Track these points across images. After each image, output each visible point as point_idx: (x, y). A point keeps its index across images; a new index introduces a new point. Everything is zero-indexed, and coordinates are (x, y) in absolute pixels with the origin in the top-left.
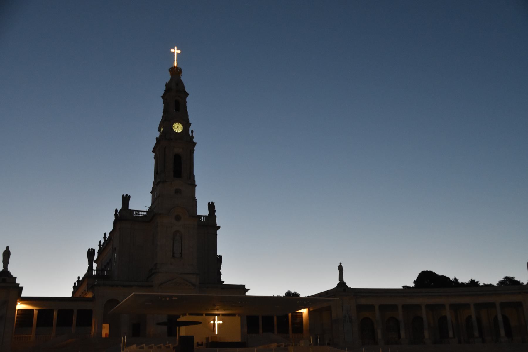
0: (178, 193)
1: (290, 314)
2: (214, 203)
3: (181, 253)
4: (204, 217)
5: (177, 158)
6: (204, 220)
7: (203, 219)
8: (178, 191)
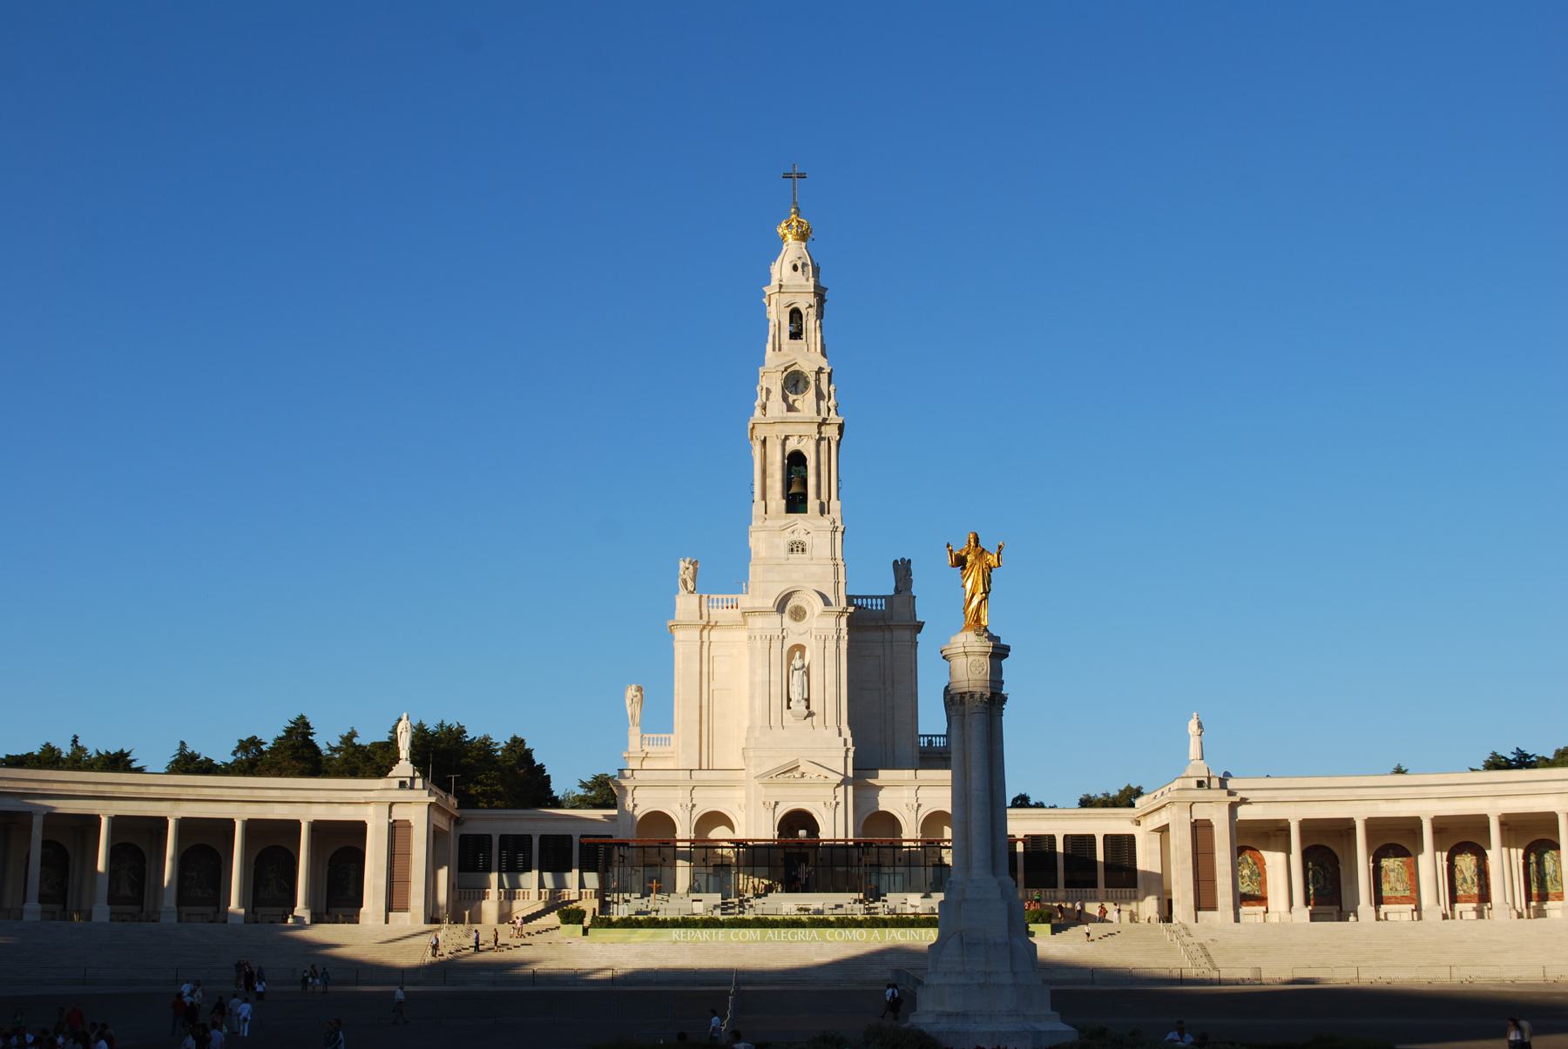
0: (798, 551)
1: (467, 913)
2: (909, 561)
3: (808, 700)
4: (883, 600)
6: (884, 608)
7: (881, 605)
8: (797, 547)
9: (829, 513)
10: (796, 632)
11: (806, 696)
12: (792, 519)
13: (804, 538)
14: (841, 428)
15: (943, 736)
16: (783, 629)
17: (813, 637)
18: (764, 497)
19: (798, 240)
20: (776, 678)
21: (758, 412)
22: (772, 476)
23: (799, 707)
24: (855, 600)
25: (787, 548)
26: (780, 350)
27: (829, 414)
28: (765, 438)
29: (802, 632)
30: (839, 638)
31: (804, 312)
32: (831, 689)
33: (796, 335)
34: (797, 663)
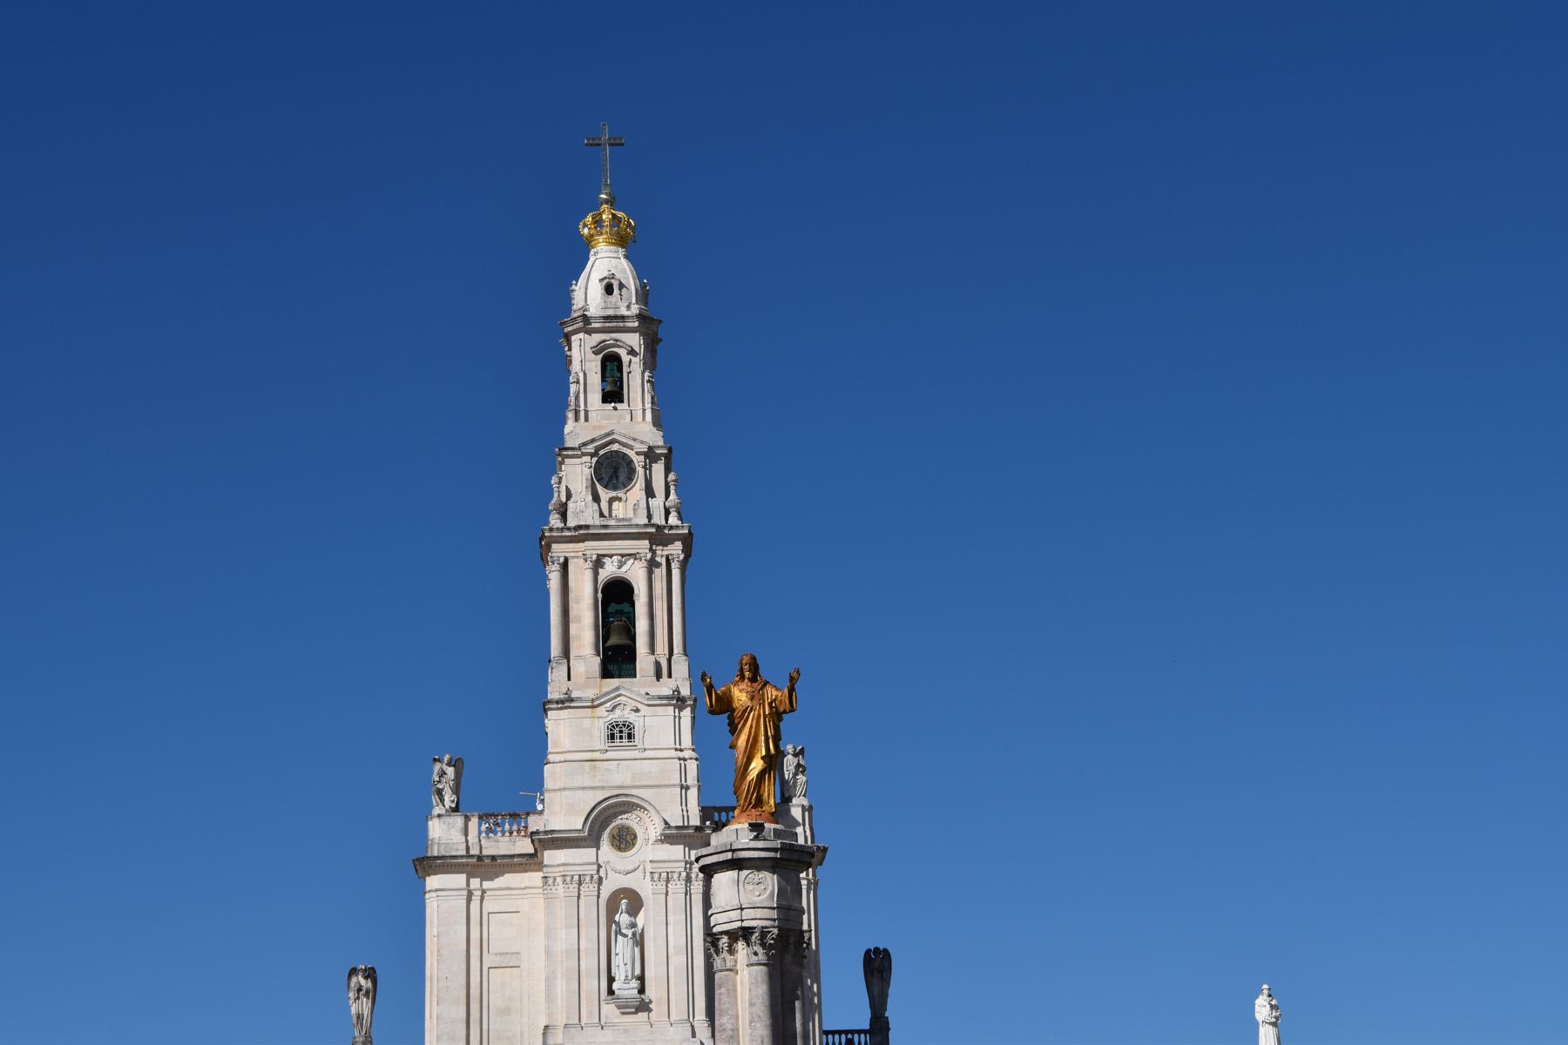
0: (621, 738)
3: (641, 978)
5: (616, 596)
8: (621, 733)
9: (670, 676)
10: (619, 869)
11: (638, 972)
12: (614, 686)
13: (632, 718)
14: (687, 541)
15: (865, 1032)
16: (599, 867)
17: (648, 875)
18: (566, 653)
19: (612, 244)
20: (589, 942)
21: (555, 521)
22: (579, 620)
23: (625, 988)
24: (716, 814)
25: (604, 733)
26: (586, 419)
27: (667, 520)
28: (566, 560)
29: (631, 868)
30: (688, 880)
31: (625, 358)
32: (679, 960)
33: (613, 394)
34: (623, 918)
